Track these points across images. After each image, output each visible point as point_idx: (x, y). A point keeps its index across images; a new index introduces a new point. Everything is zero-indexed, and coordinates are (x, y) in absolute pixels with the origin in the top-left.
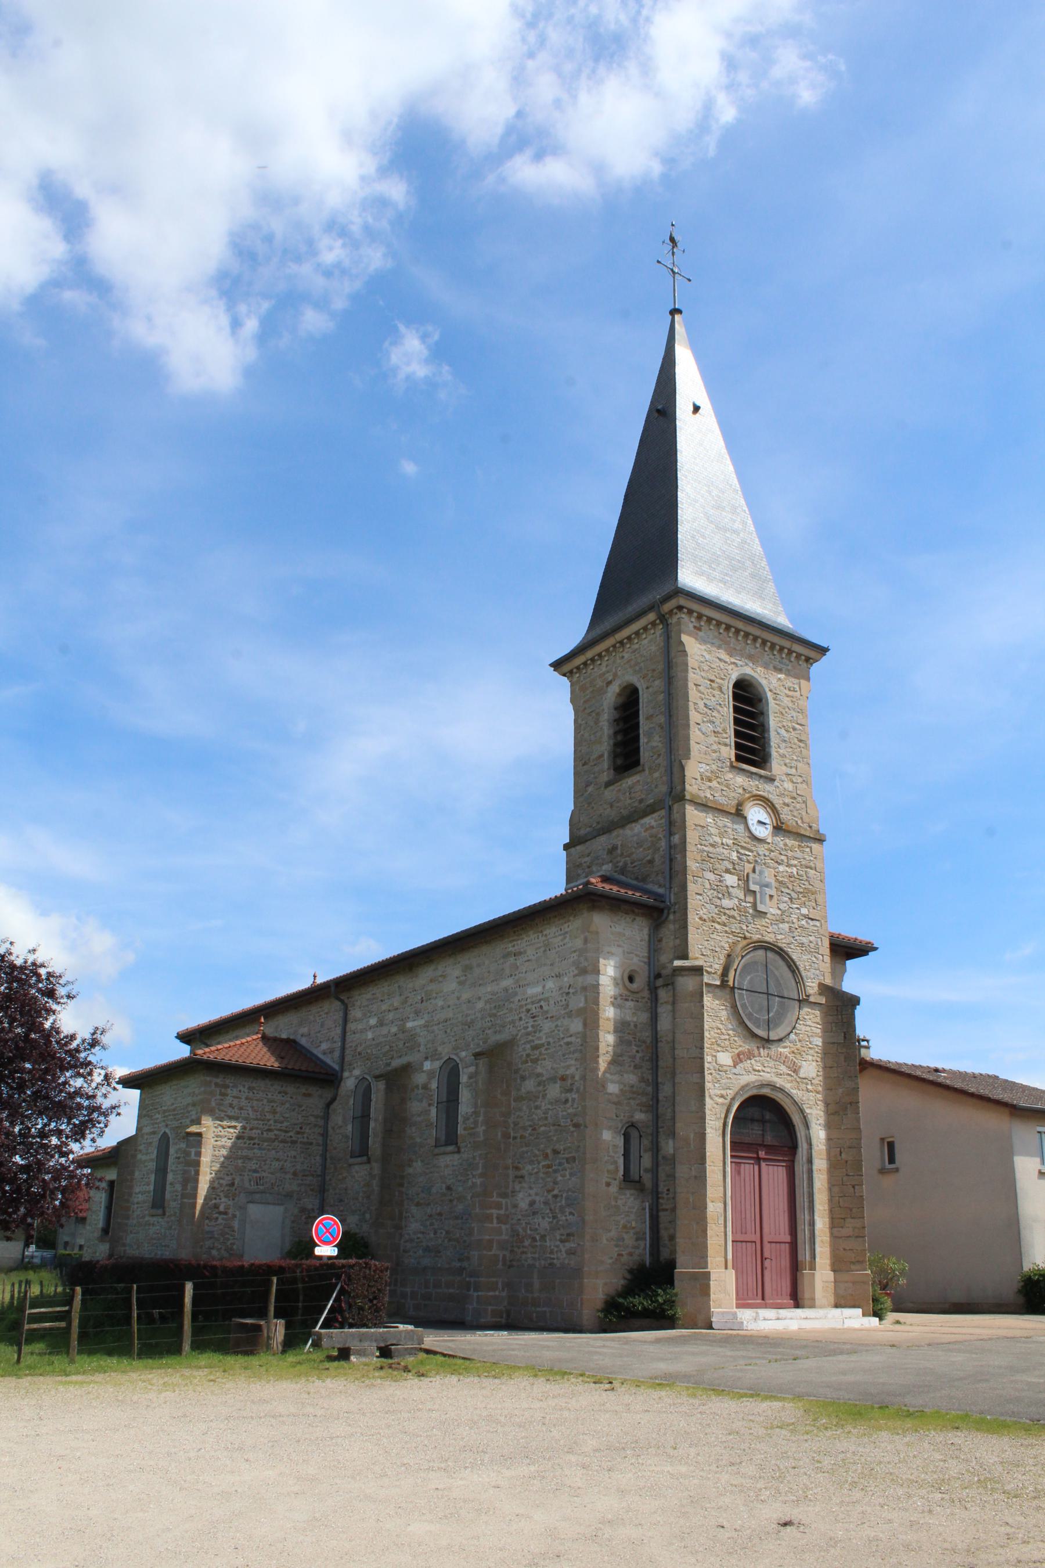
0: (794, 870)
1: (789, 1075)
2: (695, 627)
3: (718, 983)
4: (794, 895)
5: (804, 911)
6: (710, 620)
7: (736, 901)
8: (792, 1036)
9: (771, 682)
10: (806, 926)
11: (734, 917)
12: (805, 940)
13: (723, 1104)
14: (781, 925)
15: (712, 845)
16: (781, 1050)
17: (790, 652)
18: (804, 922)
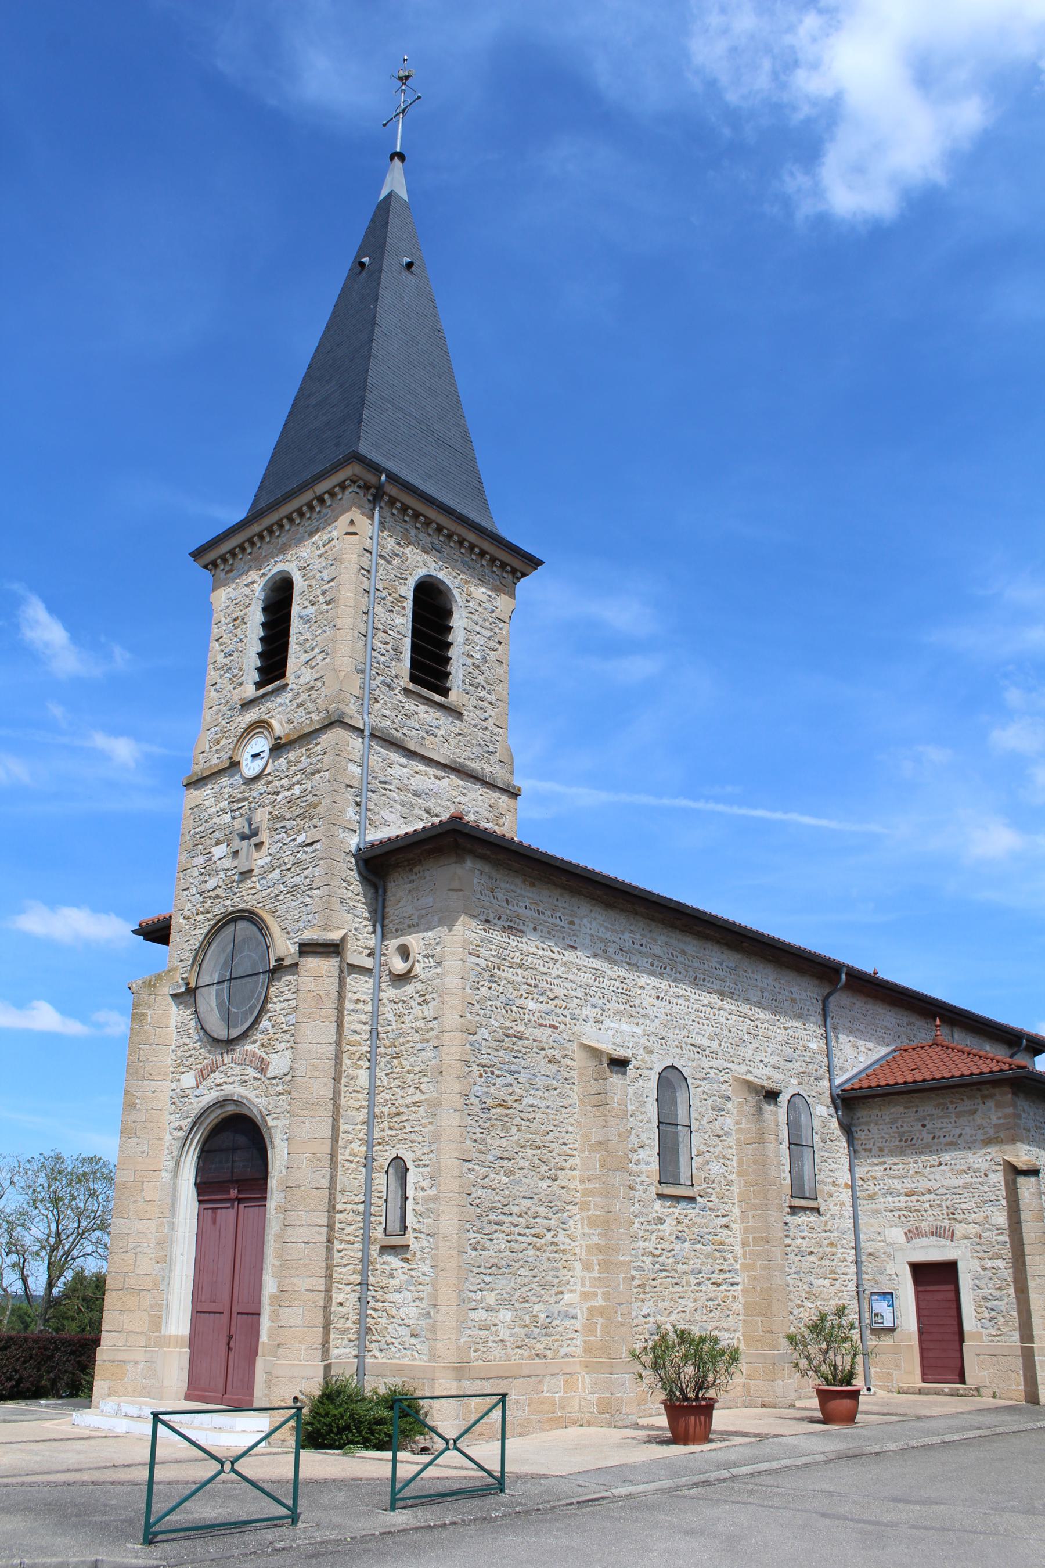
0: (297, 790)
1: (255, 1079)
2: (227, 573)
3: (183, 989)
4: (289, 824)
5: (300, 839)
6: (232, 553)
7: (222, 874)
8: (265, 1023)
9: (287, 564)
10: (304, 857)
11: (218, 897)
12: (297, 879)
13: (179, 1138)
14: (271, 876)
15: (206, 822)
16: (249, 1048)
17: (321, 500)
18: (299, 855)
